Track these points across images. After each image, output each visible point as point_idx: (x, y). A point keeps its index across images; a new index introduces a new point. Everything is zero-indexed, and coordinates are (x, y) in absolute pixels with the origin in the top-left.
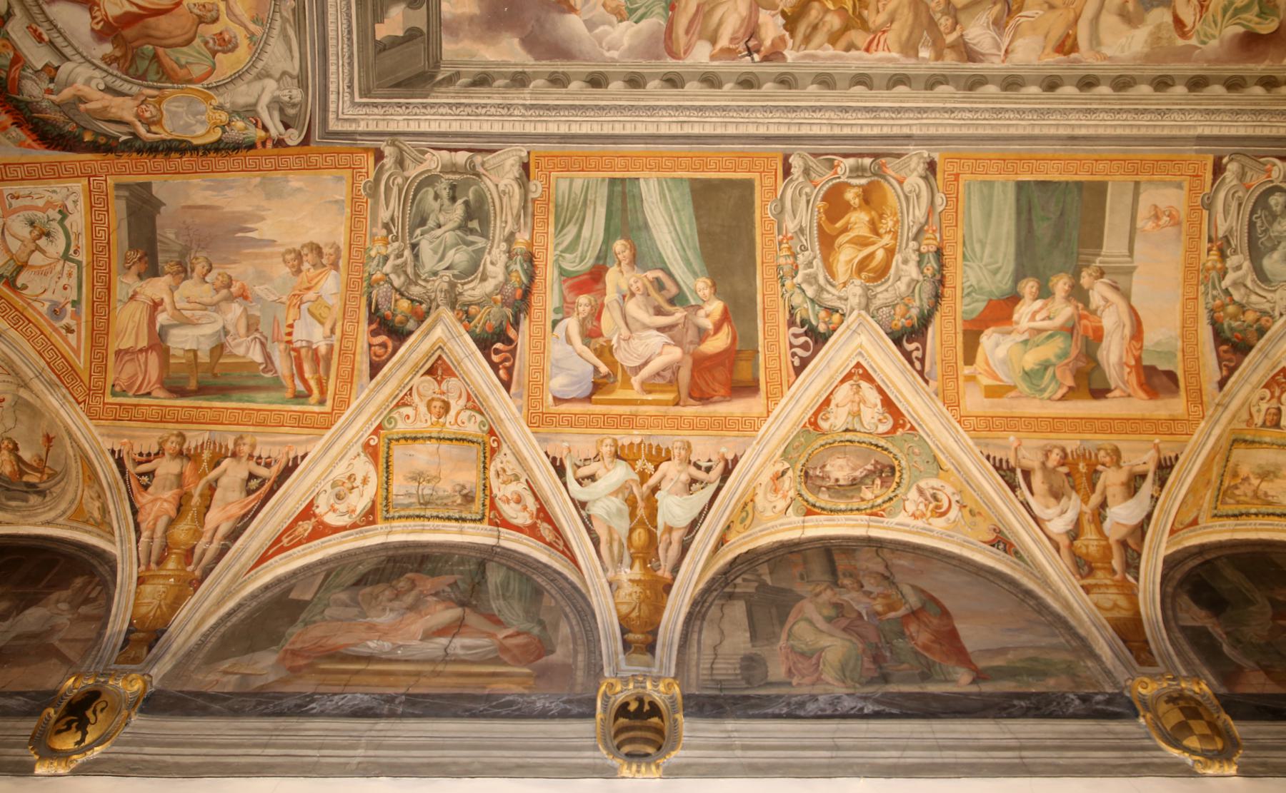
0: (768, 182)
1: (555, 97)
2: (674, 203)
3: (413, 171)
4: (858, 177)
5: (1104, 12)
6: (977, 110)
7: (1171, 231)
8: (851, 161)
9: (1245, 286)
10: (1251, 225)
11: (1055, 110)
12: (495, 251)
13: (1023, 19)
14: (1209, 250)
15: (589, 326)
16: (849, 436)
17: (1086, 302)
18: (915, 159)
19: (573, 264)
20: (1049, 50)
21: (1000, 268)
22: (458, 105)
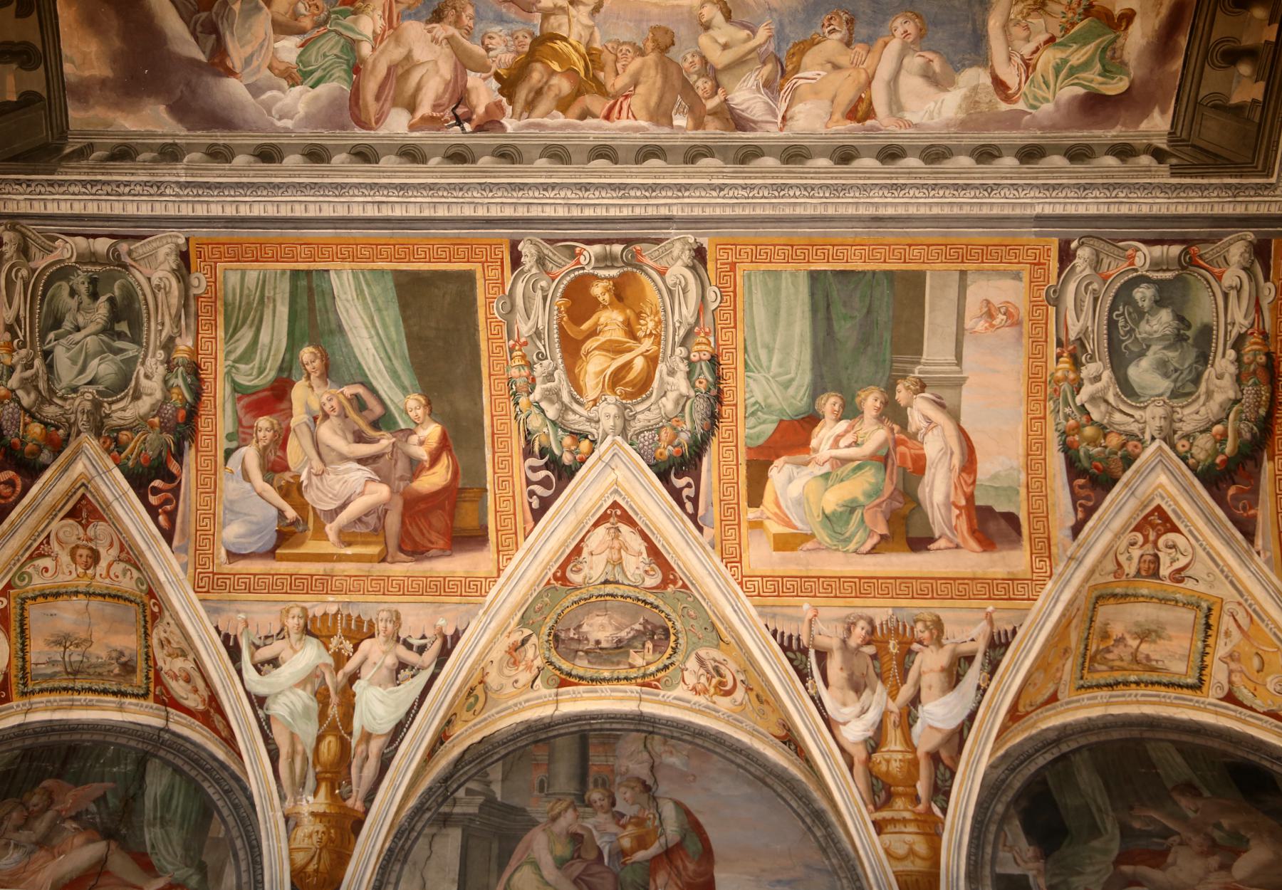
0: (493, 274)
1: (216, 174)
2: (374, 301)
3: (40, 262)
4: (607, 267)
5: (903, 72)
6: (752, 187)
7: (1009, 332)
8: (597, 248)
9: (1106, 402)
10: (1112, 324)
11: (852, 186)
12: (150, 361)
13: (801, 82)
14: (1059, 356)
15: (272, 457)
16: (609, 589)
17: (904, 424)
18: (678, 246)
19: (249, 377)
20: (837, 116)
21: (792, 380)
22: (94, 183)
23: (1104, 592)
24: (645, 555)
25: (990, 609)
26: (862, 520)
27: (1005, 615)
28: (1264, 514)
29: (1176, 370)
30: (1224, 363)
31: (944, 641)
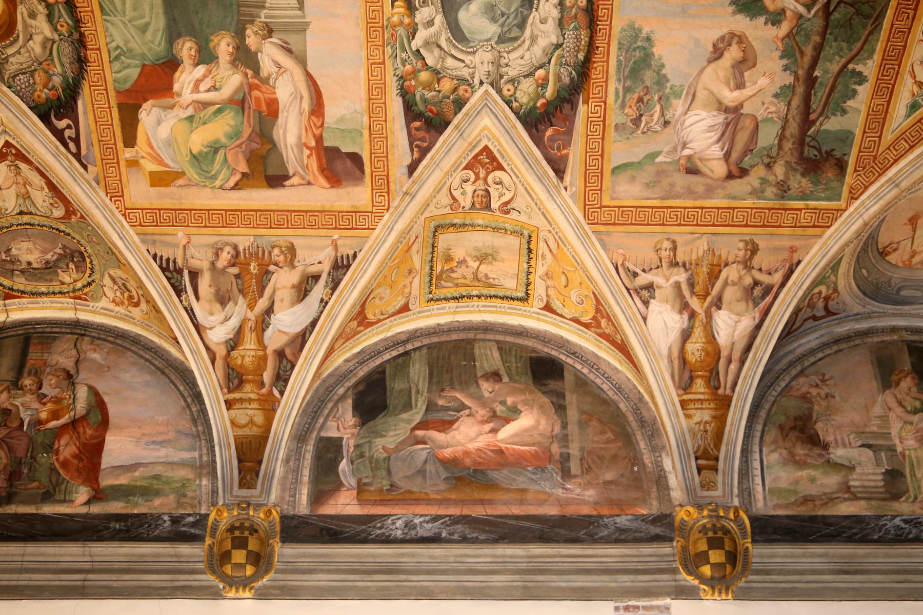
16: (26, 219)
17: (257, 70)
21: (147, 25)
23: (442, 222)
24: (46, 190)
25: (336, 237)
26: (226, 160)
27: (348, 241)
28: (576, 154)
31: (296, 264)
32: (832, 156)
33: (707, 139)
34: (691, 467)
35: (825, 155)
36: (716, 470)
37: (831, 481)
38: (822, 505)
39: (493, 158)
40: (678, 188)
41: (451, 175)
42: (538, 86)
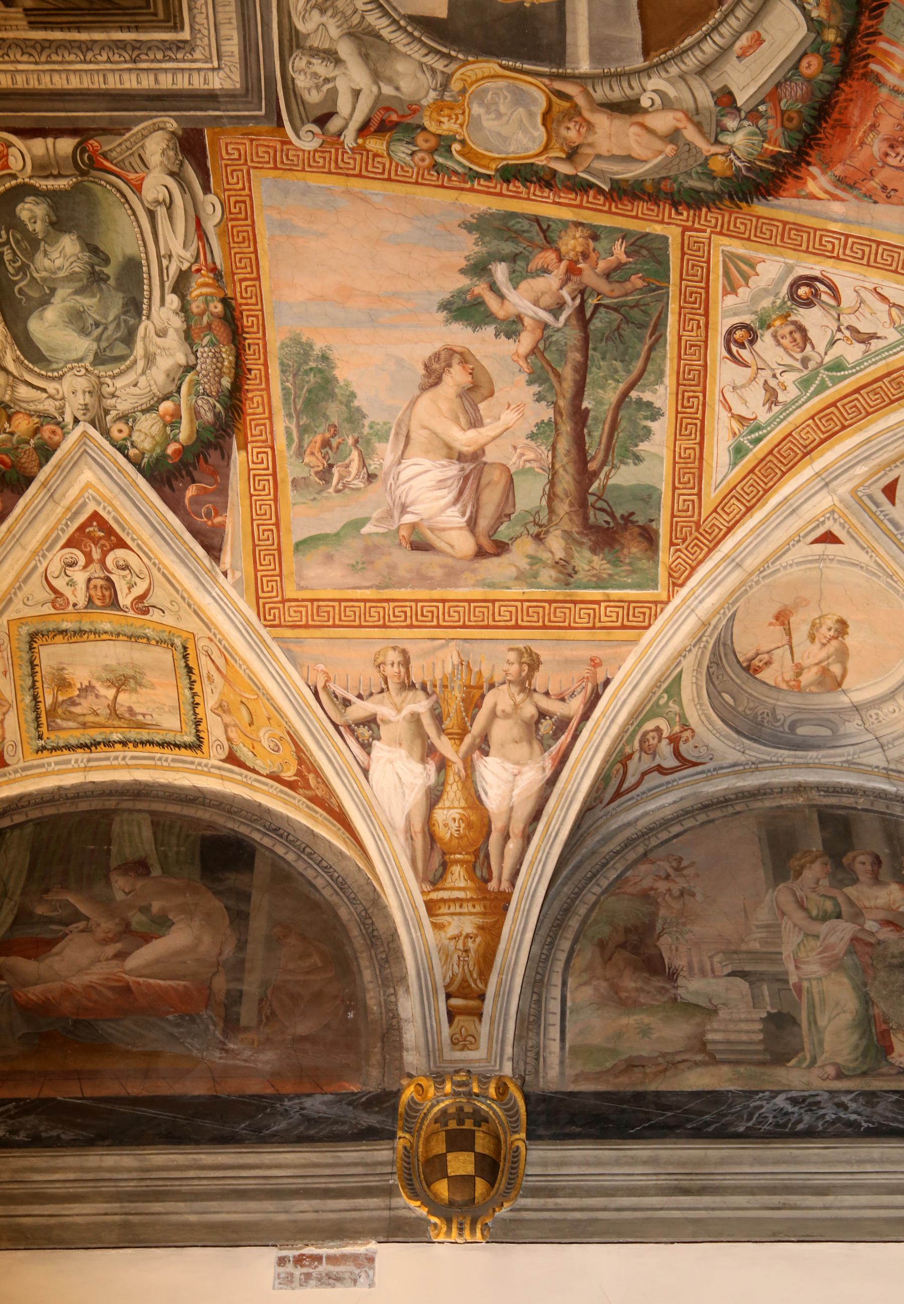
23: (42, 627)
28: (236, 522)
29: (97, 325)
30: (164, 313)
32: (633, 522)
33: (437, 499)
34: (437, 1010)
35: (622, 522)
36: (480, 1016)
37: (674, 1033)
38: (656, 1074)
39: (109, 531)
40: (402, 572)
41: (44, 556)
42: (165, 426)
